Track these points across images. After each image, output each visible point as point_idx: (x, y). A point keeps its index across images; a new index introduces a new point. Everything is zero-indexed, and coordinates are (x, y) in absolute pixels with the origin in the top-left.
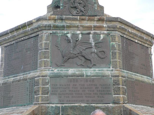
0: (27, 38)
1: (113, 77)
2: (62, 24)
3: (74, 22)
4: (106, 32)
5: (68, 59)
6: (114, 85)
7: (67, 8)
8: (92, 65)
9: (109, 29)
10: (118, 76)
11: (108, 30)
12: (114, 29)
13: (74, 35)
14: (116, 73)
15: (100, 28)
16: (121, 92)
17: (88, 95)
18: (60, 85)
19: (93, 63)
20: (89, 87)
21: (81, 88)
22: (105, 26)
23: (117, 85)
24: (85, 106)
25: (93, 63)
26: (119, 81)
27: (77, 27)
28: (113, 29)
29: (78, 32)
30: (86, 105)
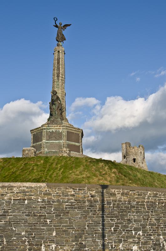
13: (53, 131)
14: (64, 142)
27: (53, 129)
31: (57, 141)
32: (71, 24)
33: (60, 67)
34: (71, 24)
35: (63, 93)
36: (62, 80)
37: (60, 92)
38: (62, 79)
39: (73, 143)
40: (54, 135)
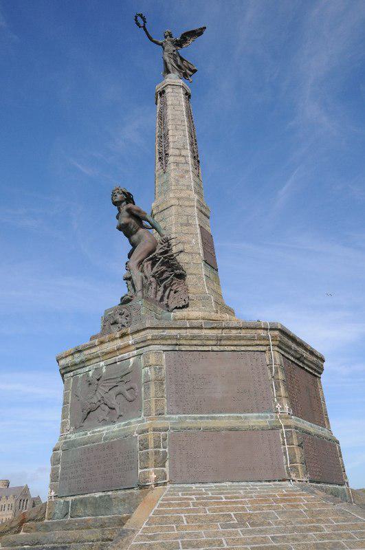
2: (79, 360)
3: (93, 350)
4: (135, 352)
5: (89, 413)
6: (141, 450)
9: (138, 346)
10: (147, 431)
11: (137, 349)
12: (145, 343)
14: (147, 423)
16: (151, 462)
19: (118, 413)
22: (130, 342)
24: (100, 497)
26: (146, 440)
29: (102, 364)
30: (101, 494)
31: (115, 428)
32: (205, 28)
33: (170, 127)
34: (205, 28)
35: (187, 203)
36: (177, 164)
37: (173, 202)
38: (182, 159)
39: (224, 420)
40: (102, 390)
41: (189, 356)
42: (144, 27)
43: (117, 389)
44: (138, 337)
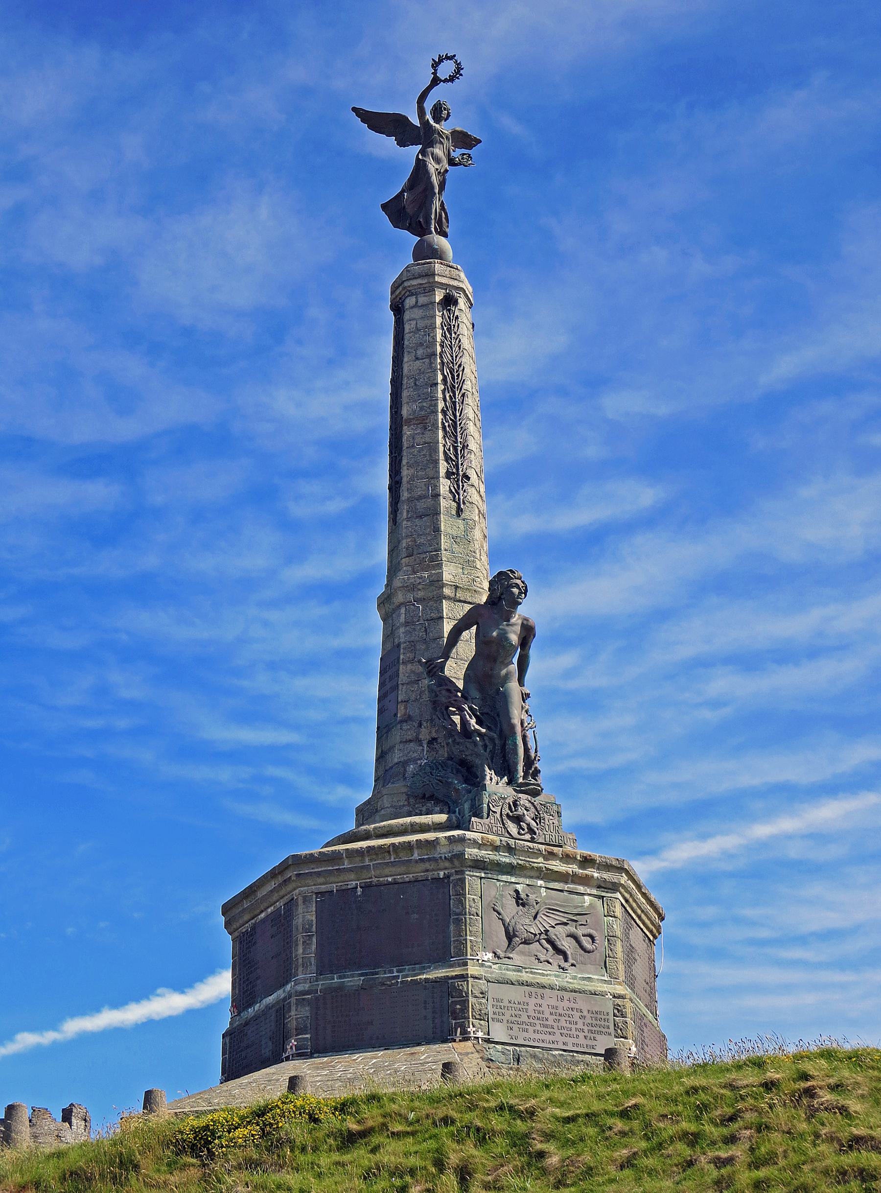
0: (407, 880)
1: (614, 997)
4: (594, 892)
7: (498, 815)
8: (569, 964)
15: (585, 881)
17: (565, 1032)
18: (510, 1002)
20: (567, 1012)
21: (551, 1014)
23: (623, 1016)
25: (571, 961)
28: (611, 887)
41: (629, 919)
42: (436, 81)
43: (571, 928)
44: (607, 876)
